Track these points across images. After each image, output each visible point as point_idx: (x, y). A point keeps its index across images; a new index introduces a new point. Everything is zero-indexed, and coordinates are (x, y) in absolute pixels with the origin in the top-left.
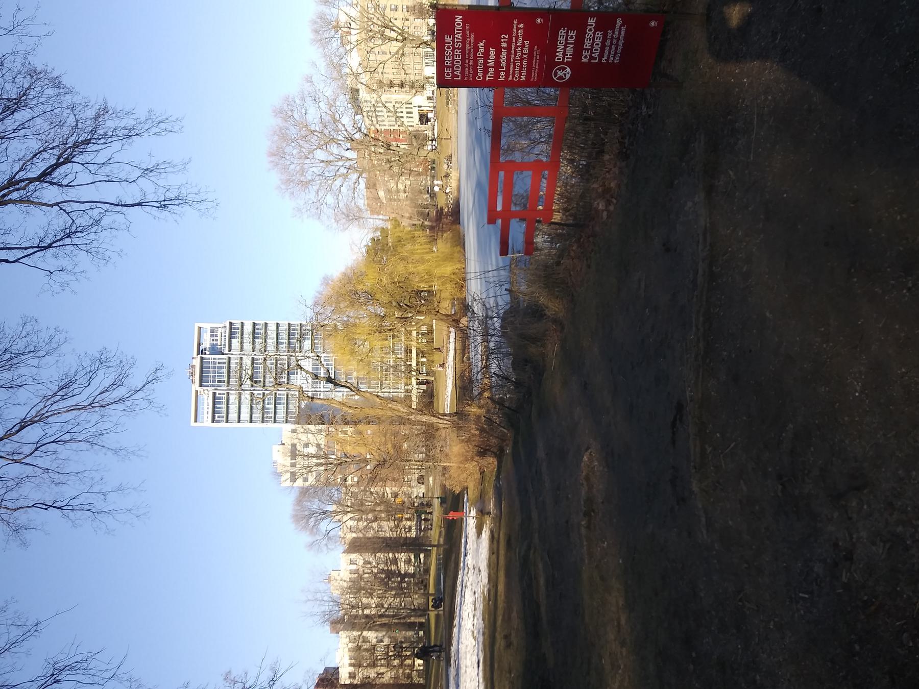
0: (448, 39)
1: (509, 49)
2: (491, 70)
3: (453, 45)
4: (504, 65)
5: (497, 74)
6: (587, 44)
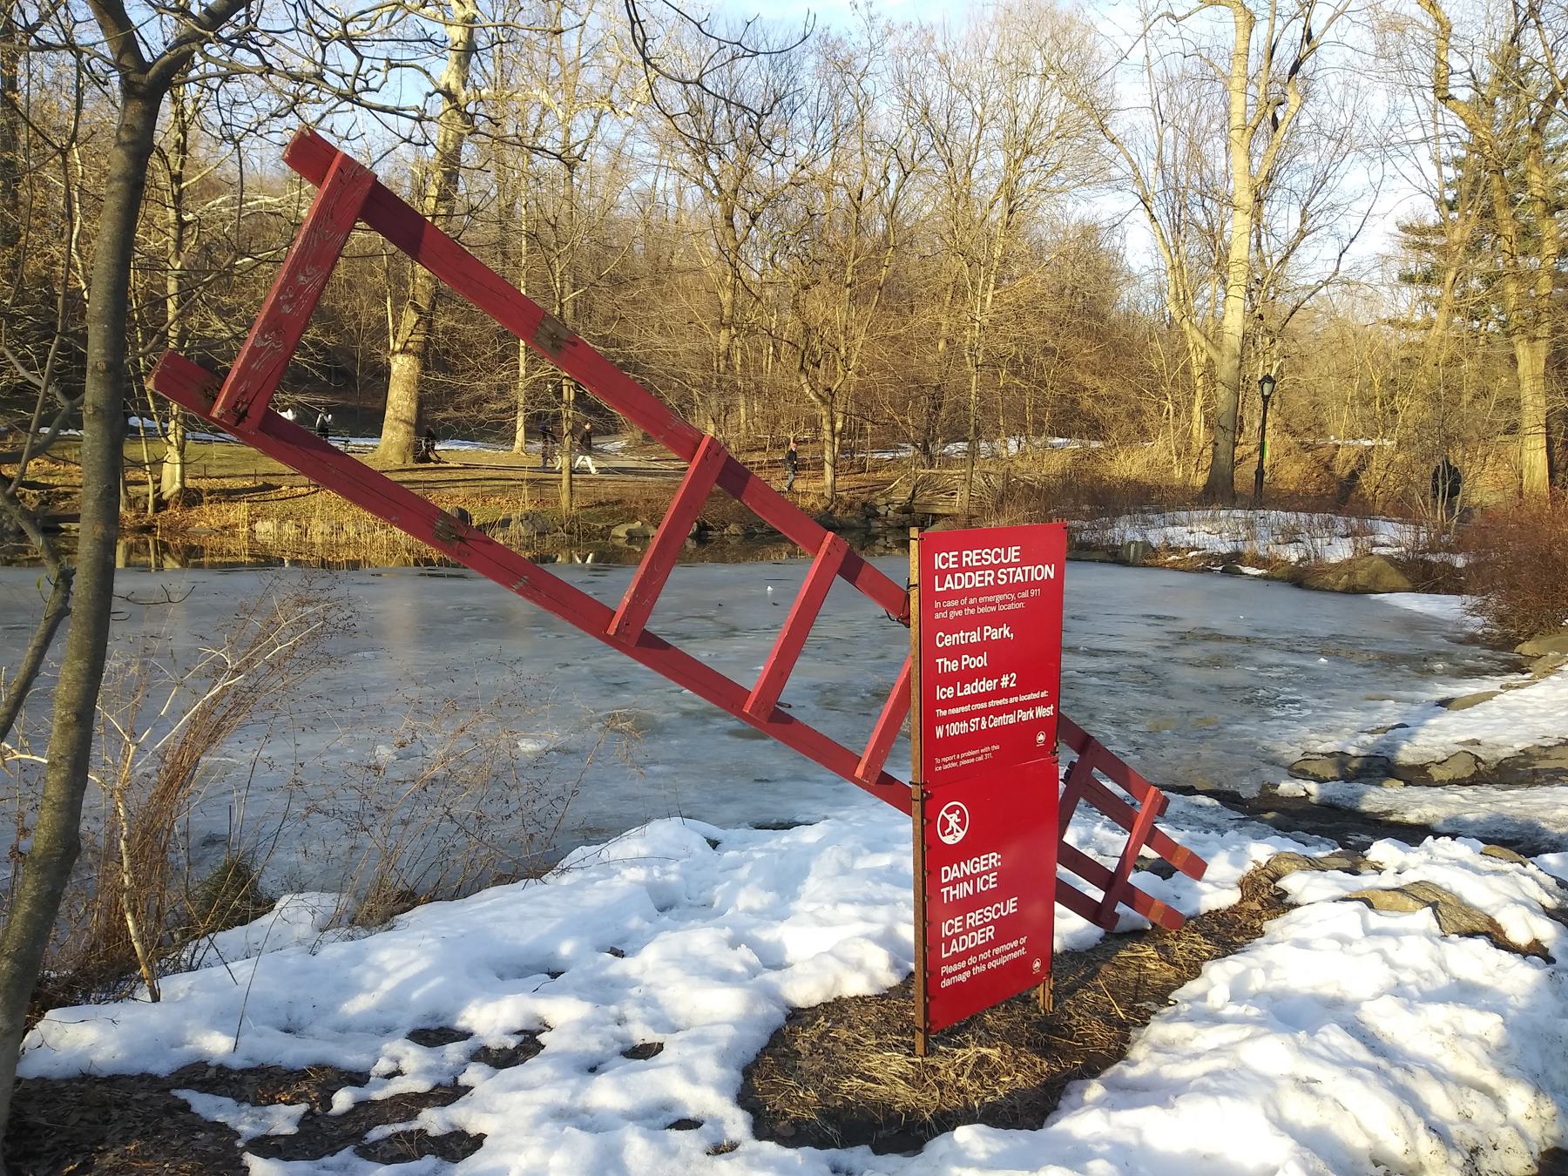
0: (1013, 552)
2: (953, 666)
3: (1001, 565)
4: (969, 690)
6: (974, 918)
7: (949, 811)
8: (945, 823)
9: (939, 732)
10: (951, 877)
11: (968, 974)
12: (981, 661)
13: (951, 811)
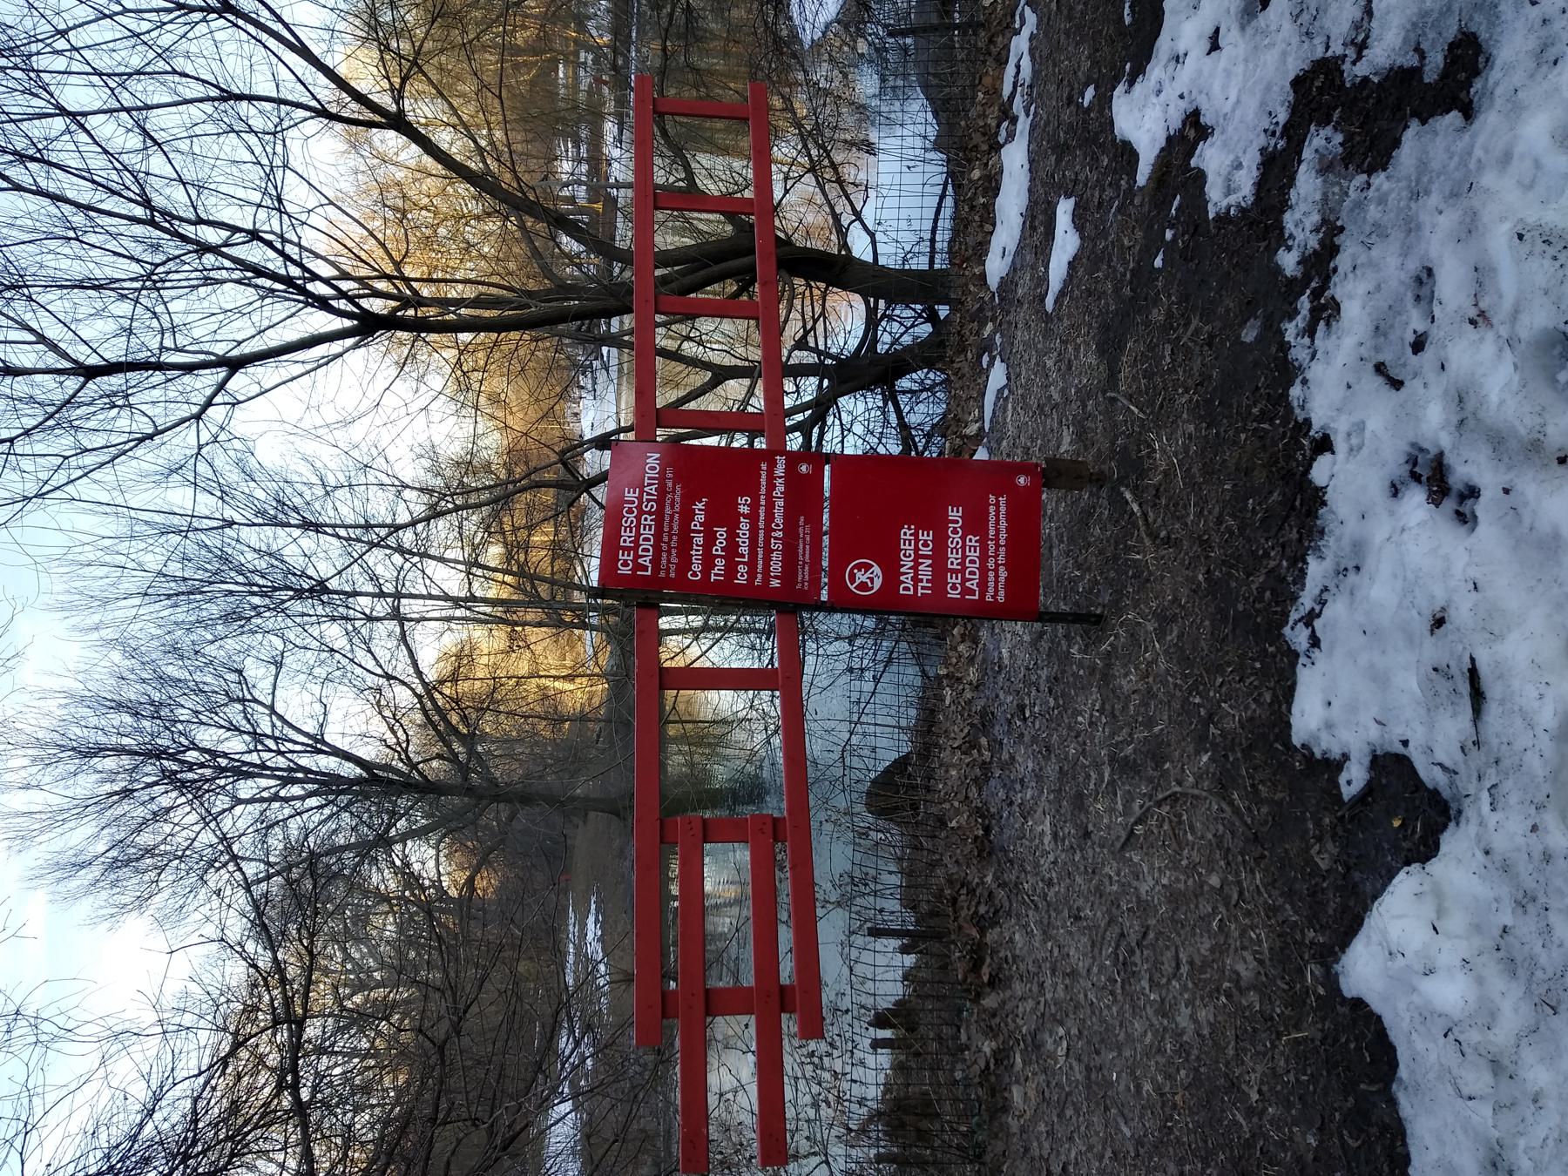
1: (753, 517)
2: (720, 563)
4: (744, 549)
5: (731, 570)
6: (953, 560)
7: (853, 580)
8: (863, 587)
9: (775, 583)
10: (910, 583)
11: (1002, 569)
12: (721, 533)
13: (853, 578)
